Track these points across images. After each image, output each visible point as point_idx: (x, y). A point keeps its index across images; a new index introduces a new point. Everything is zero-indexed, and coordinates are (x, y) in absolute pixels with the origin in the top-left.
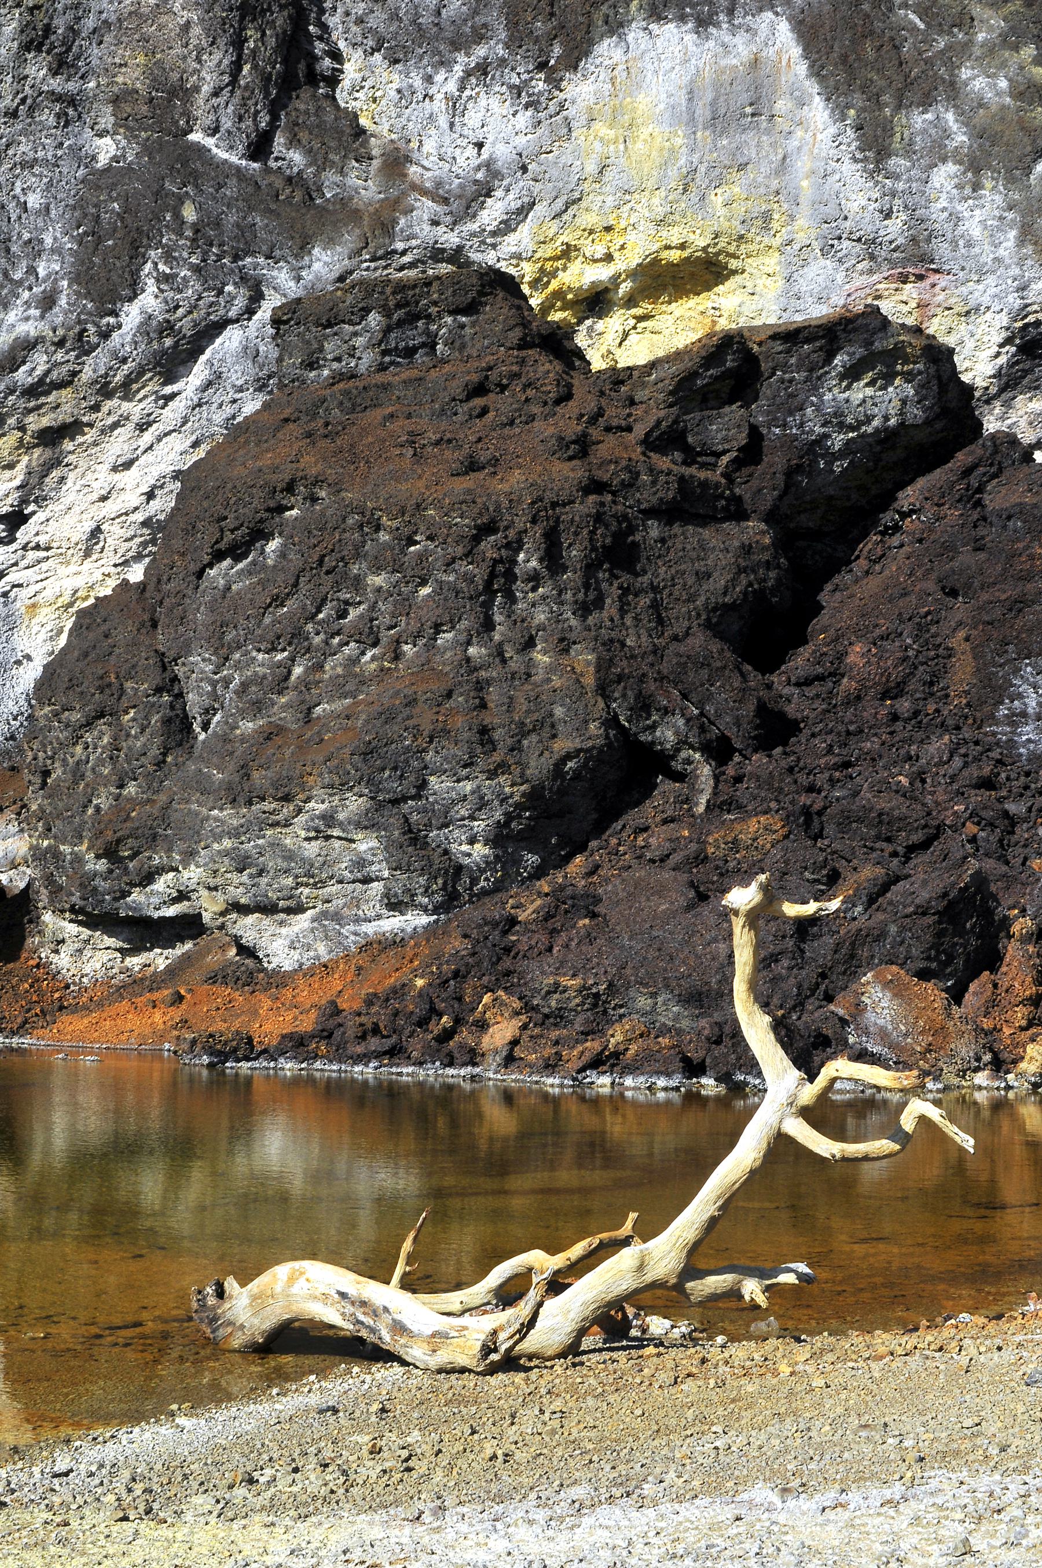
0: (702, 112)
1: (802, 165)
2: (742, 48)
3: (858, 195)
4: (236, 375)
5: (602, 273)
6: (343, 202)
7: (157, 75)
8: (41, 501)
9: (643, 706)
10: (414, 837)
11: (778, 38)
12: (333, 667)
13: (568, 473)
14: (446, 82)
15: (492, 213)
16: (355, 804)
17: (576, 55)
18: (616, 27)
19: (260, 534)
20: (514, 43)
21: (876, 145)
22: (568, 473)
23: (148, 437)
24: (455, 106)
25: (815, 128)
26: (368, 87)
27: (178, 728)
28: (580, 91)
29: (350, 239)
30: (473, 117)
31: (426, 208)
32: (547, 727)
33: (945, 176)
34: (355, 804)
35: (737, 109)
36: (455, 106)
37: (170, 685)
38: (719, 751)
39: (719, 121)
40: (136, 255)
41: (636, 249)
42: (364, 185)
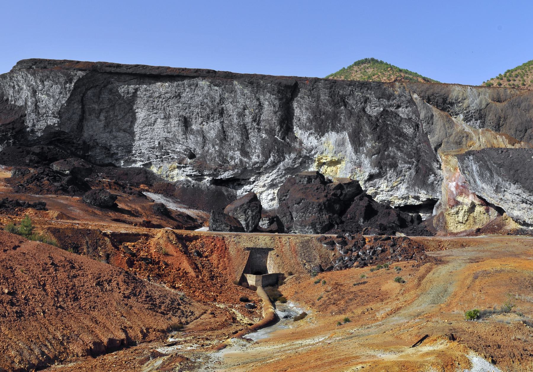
0: (337, 144)
1: (348, 152)
2: (342, 136)
3: (354, 157)
4: (282, 168)
5: (325, 161)
6: (295, 147)
7: (271, 128)
8: (257, 180)
9: (332, 221)
10: (315, 230)
11: (346, 135)
12: (307, 215)
13: (325, 199)
14: (307, 134)
15: (313, 152)
16: (310, 227)
17: (323, 135)
18: (328, 132)
19: (300, 203)
20: (315, 131)
21: (356, 151)
22: (325, 199)
23: (271, 174)
24: (309, 137)
25: (349, 148)
26: (298, 132)
27: (292, 218)
28: (323, 139)
29: (296, 153)
30: (310, 139)
31: (305, 151)
32: (325, 222)
33: (363, 156)
34: (310, 227)
35: (341, 144)
36: (309, 137)
37: (291, 214)
38: (338, 224)
39: (339, 146)
40: (270, 153)
41: (329, 159)
42: (297, 145)
